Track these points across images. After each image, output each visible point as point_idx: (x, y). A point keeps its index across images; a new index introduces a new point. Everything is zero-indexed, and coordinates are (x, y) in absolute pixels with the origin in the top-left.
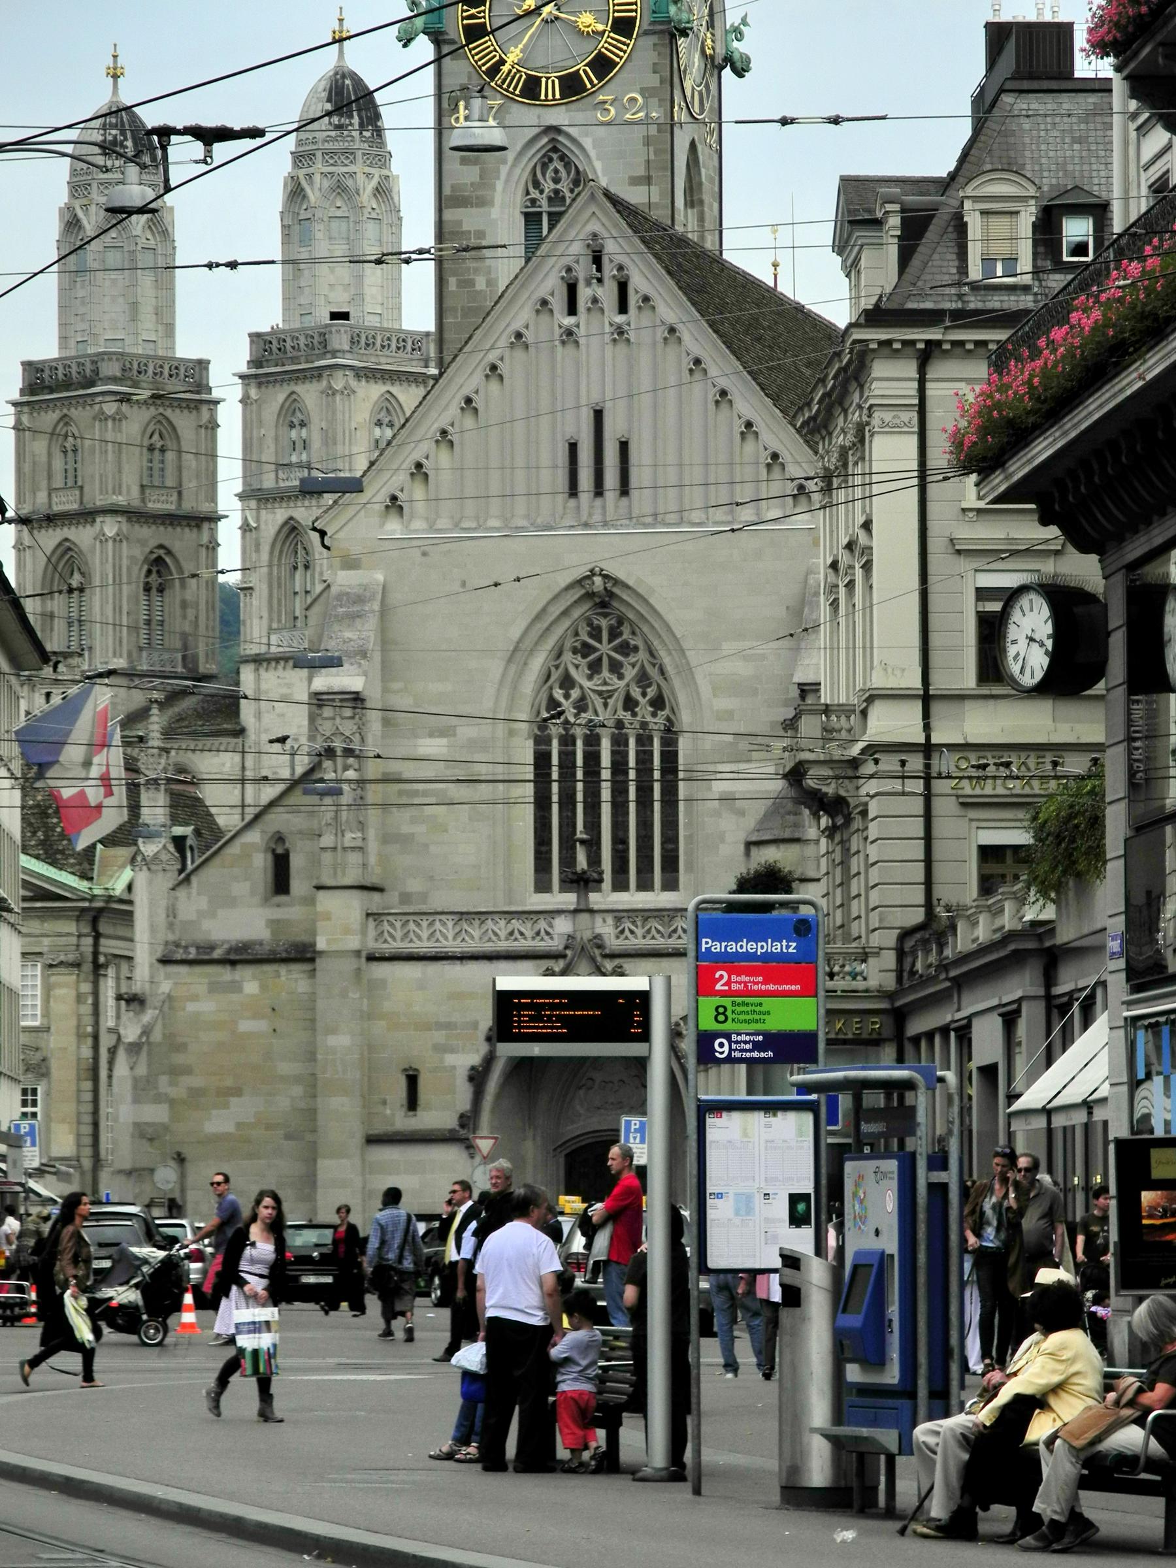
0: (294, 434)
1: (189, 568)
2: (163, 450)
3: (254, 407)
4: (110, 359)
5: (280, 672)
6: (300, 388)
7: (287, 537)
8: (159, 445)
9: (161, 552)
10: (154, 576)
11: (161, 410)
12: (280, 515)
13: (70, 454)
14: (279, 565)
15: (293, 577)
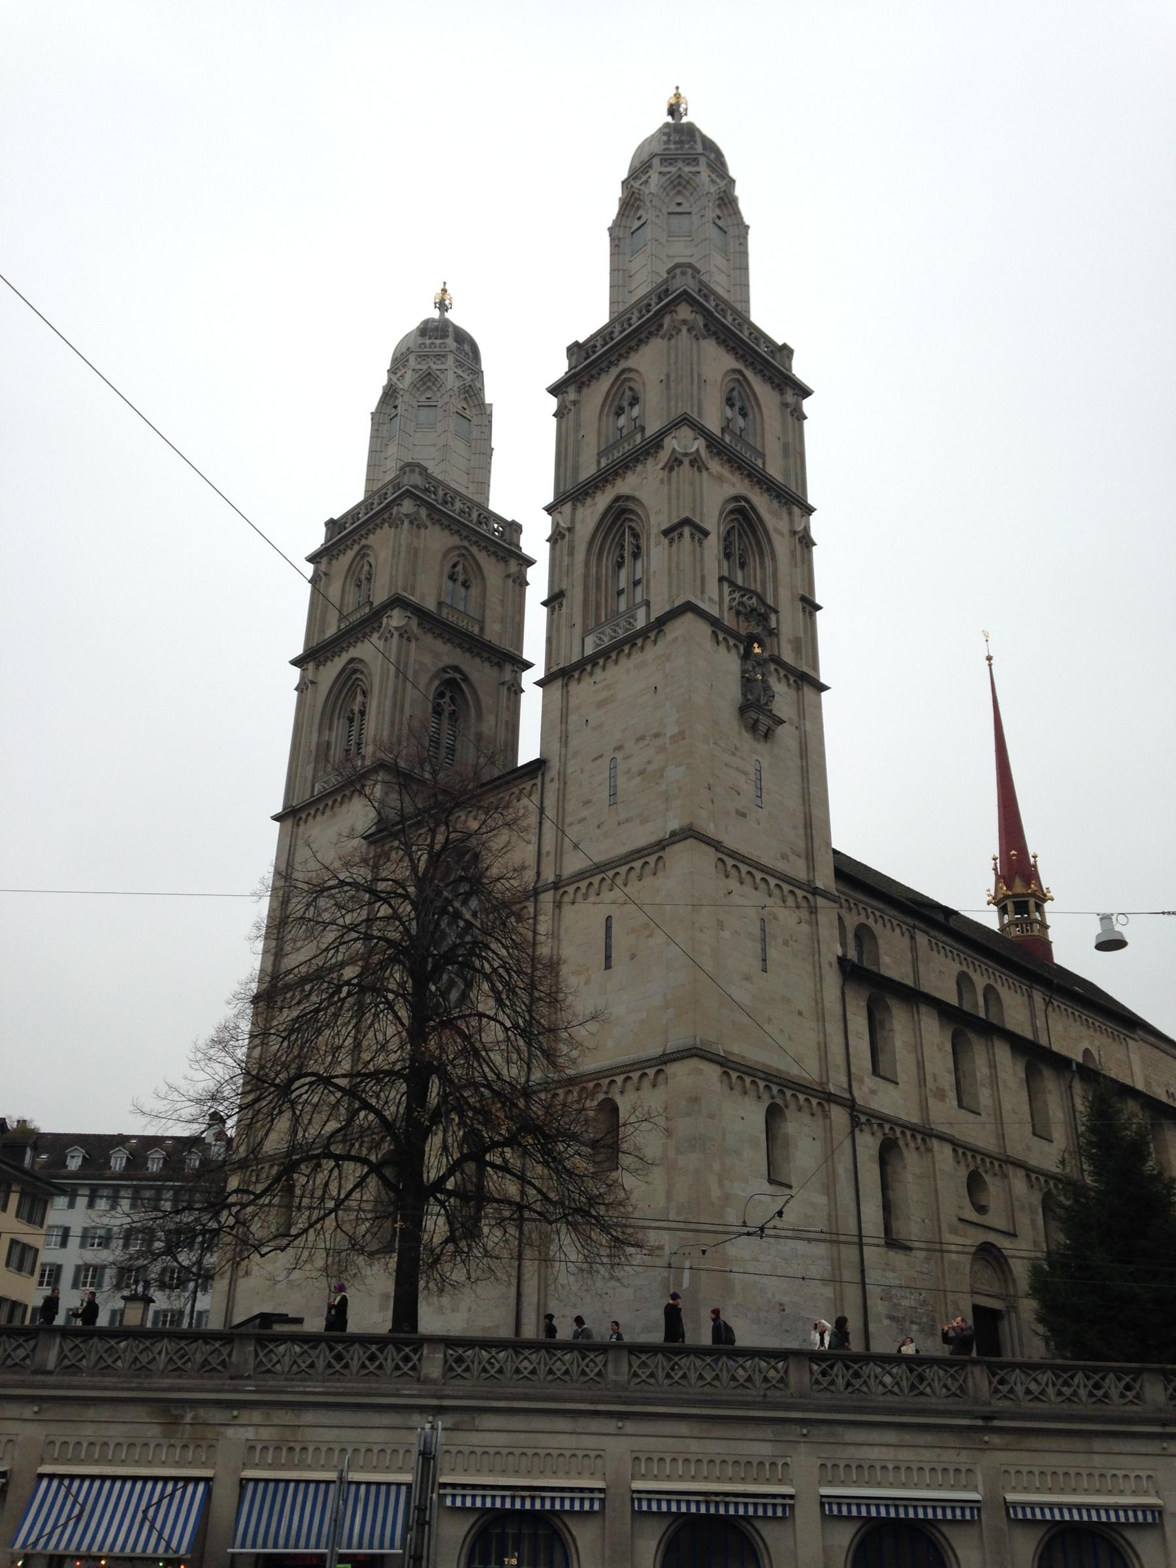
0: (622, 421)
1: (486, 701)
2: (466, 585)
3: (571, 416)
4: (412, 471)
5: (599, 674)
6: (633, 361)
7: (610, 529)
8: (461, 578)
9: (458, 676)
10: (447, 699)
11: (466, 543)
12: (602, 501)
13: (364, 582)
14: (599, 566)
15: (616, 575)
